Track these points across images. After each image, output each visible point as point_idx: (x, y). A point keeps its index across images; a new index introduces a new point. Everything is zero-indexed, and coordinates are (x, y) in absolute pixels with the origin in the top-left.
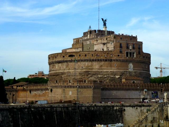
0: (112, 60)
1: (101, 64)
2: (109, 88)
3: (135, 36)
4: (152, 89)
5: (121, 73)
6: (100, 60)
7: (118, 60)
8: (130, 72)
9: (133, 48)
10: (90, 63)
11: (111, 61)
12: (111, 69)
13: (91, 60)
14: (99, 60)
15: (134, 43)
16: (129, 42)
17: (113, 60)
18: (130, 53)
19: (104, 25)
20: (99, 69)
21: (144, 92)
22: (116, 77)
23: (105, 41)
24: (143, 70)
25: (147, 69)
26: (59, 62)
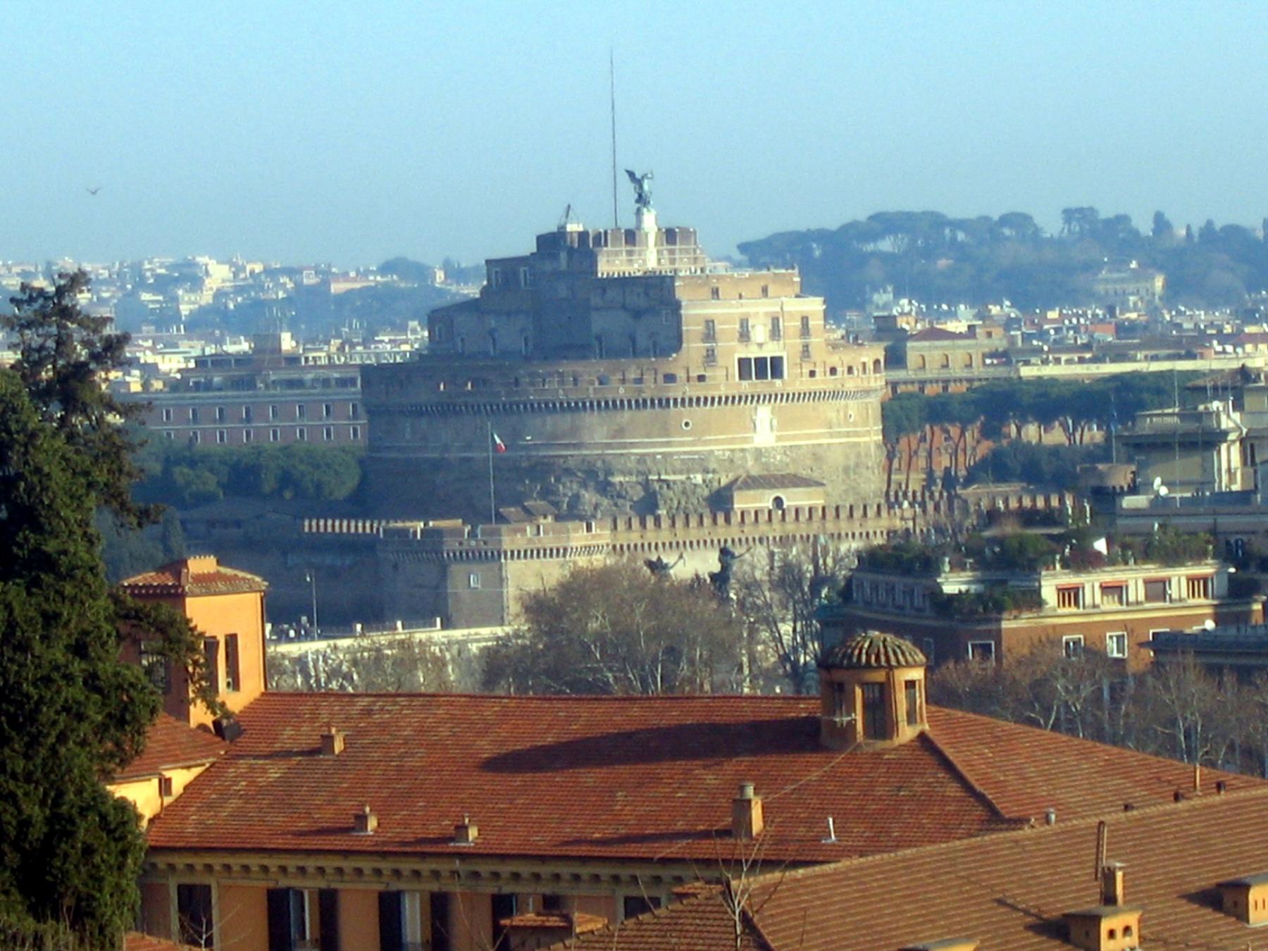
0: (668, 400)
6: (614, 402)
7: (698, 399)
8: (759, 453)
9: (775, 333)
10: (565, 421)
11: (664, 403)
12: (668, 444)
13: (569, 404)
14: (607, 403)
17: (675, 400)
18: (761, 362)
19: (638, 201)
20: (609, 446)
23: (642, 302)
24: (831, 435)
25: (855, 424)
26: (419, 412)
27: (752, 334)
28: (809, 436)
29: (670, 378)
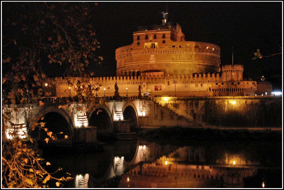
8: (151, 65)
12: (132, 64)
20: (124, 65)
27: (149, 38)
28: (166, 62)
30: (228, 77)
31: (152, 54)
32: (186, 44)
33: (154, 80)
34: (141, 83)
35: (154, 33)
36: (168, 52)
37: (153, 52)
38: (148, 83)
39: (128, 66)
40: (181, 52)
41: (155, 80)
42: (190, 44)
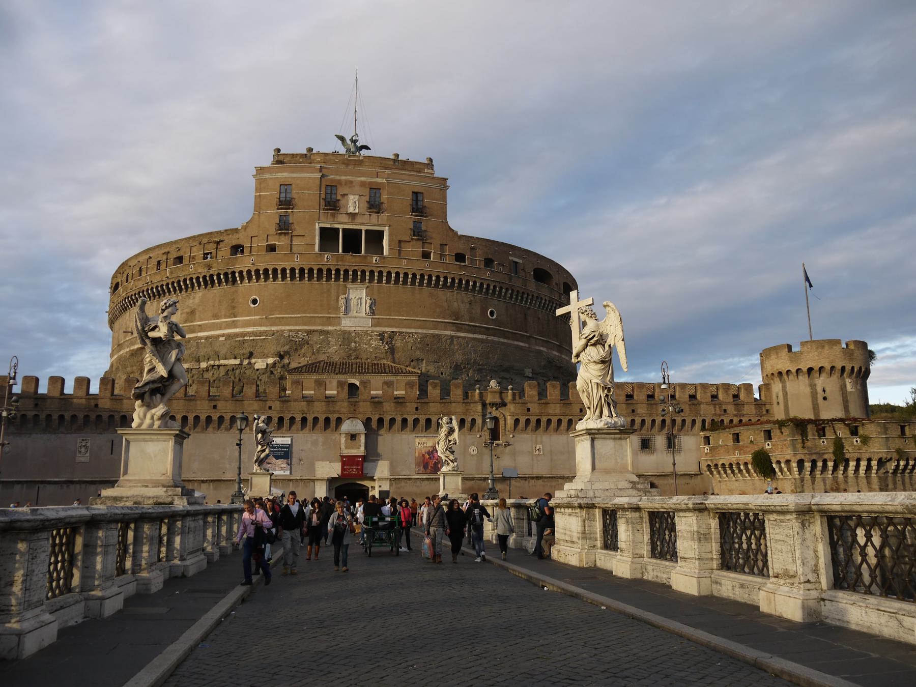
0: (233, 273)
1: (191, 301)
2: (49, 417)
3: (426, 162)
4: (410, 419)
5: (282, 340)
7: (266, 271)
8: (346, 337)
9: (374, 206)
11: (231, 278)
12: (234, 325)
15: (379, 180)
16: (343, 178)
21: (343, 440)
22: (256, 367)
24: (459, 328)
27: (342, 202)
28: (423, 325)
29: (237, 249)
30: (825, 398)
31: (354, 280)
32: (511, 258)
33: (411, 407)
34: (333, 424)
35: (370, 183)
36: (438, 277)
37: (363, 272)
38: (374, 424)
39: (207, 338)
40: (492, 287)
41: (417, 409)
42: (520, 261)
